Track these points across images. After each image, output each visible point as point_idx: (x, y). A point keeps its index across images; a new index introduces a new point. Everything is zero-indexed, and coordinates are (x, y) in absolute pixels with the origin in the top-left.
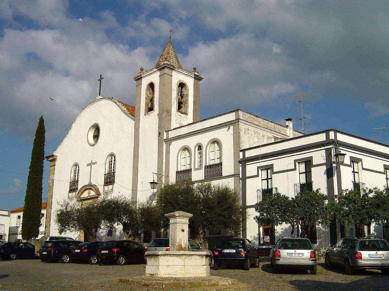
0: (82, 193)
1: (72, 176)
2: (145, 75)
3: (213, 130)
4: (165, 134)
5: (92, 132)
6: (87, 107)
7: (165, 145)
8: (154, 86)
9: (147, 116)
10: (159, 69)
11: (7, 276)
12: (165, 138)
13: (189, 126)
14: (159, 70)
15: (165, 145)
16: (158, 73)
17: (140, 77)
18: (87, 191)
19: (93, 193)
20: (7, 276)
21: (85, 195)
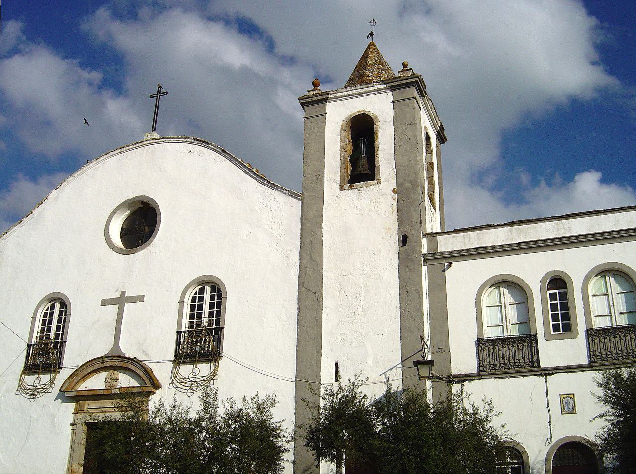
0: (84, 378)
1: (37, 333)
2: (341, 94)
3: (590, 243)
4: (424, 241)
5: (121, 219)
6: (111, 154)
7: (425, 270)
8: (373, 124)
9: (351, 193)
10: (389, 84)
11: (337, 364)
12: (425, 250)
13: (514, 228)
14: (392, 88)
15: (425, 270)
16: (389, 96)
17: (325, 97)
18: (104, 375)
19: (125, 381)
20: (337, 364)
21: (97, 382)
